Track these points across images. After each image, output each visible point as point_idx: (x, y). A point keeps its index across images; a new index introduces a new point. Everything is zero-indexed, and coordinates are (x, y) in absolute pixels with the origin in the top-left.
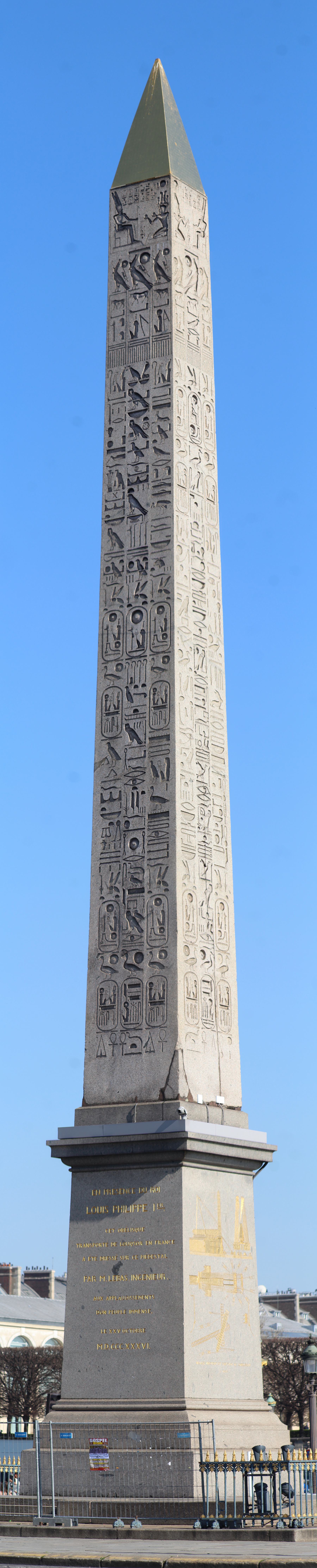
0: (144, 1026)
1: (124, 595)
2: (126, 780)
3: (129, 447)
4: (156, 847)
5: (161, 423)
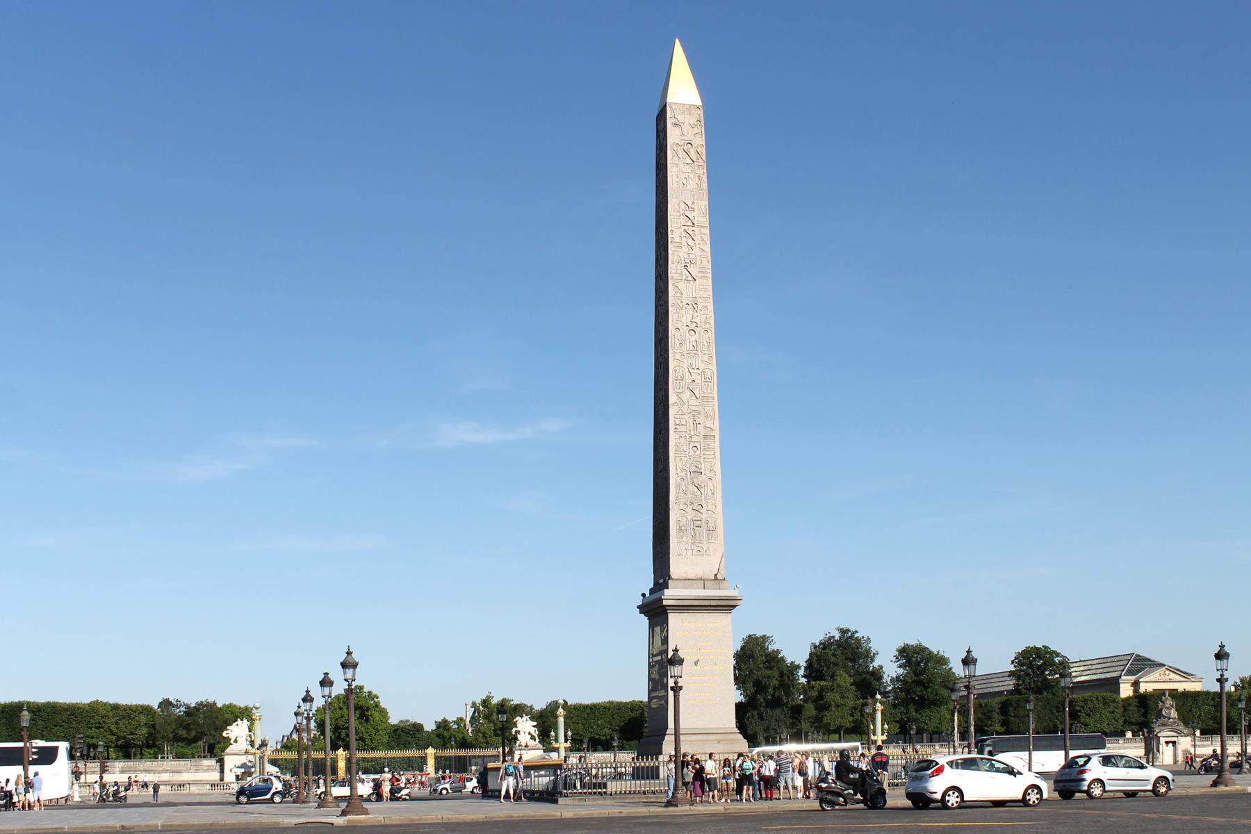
0: (704, 542)
1: (684, 320)
2: (689, 416)
3: (684, 243)
4: (708, 453)
5: (703, 236)
